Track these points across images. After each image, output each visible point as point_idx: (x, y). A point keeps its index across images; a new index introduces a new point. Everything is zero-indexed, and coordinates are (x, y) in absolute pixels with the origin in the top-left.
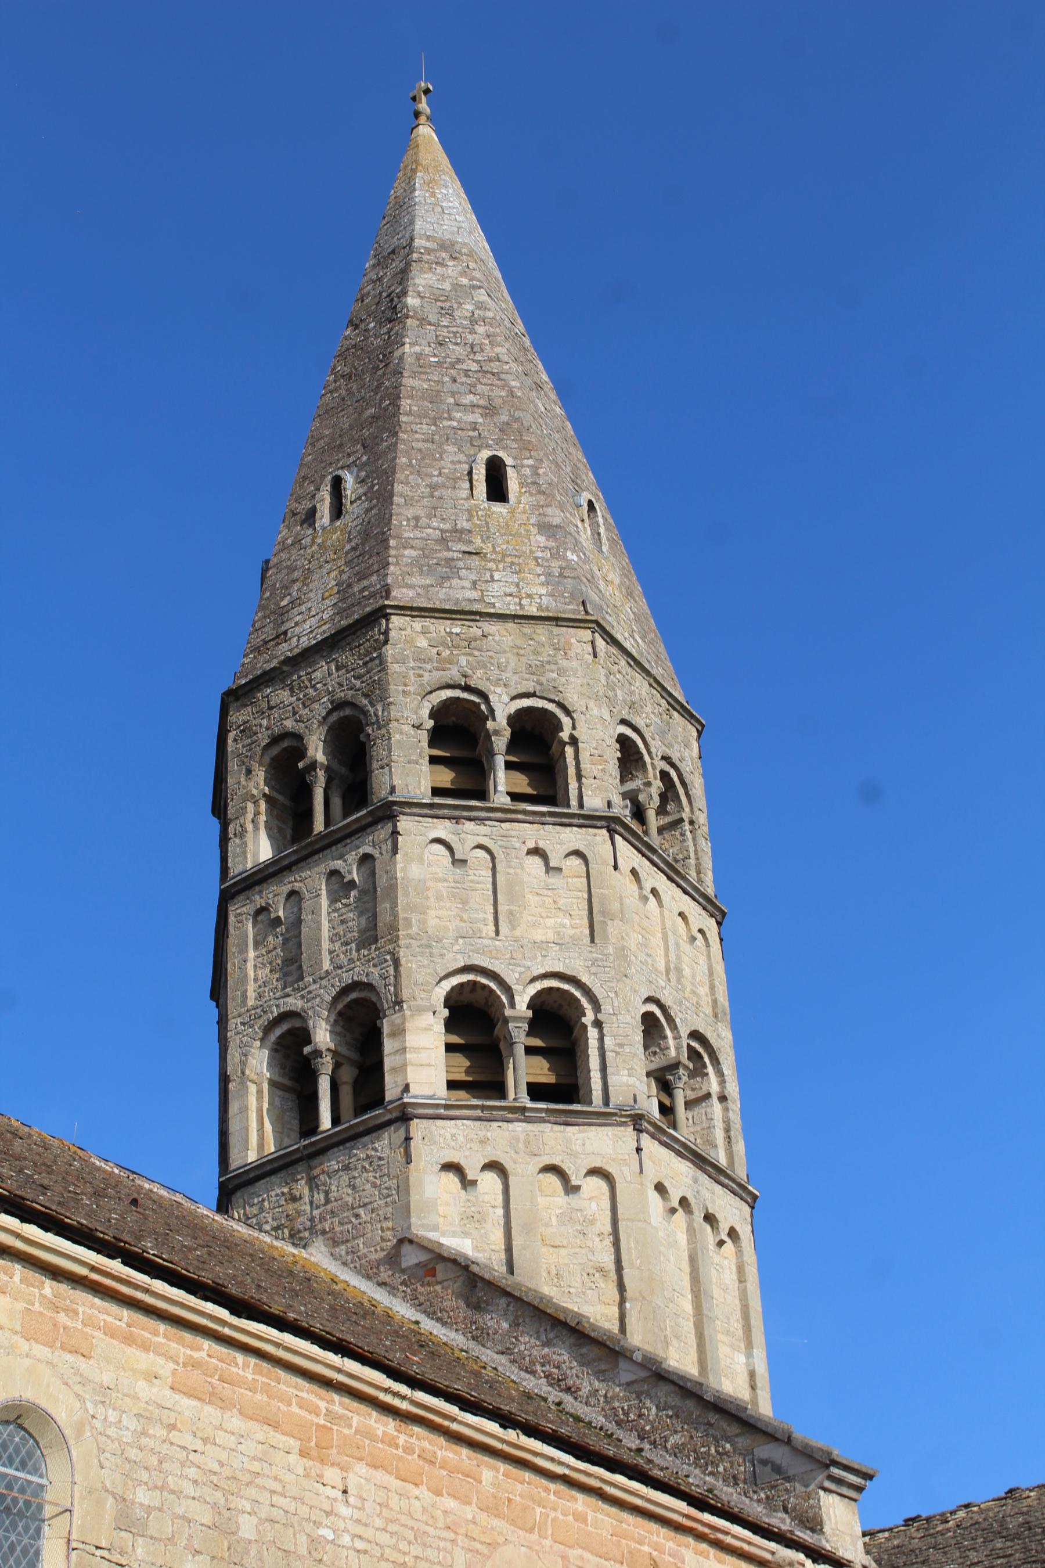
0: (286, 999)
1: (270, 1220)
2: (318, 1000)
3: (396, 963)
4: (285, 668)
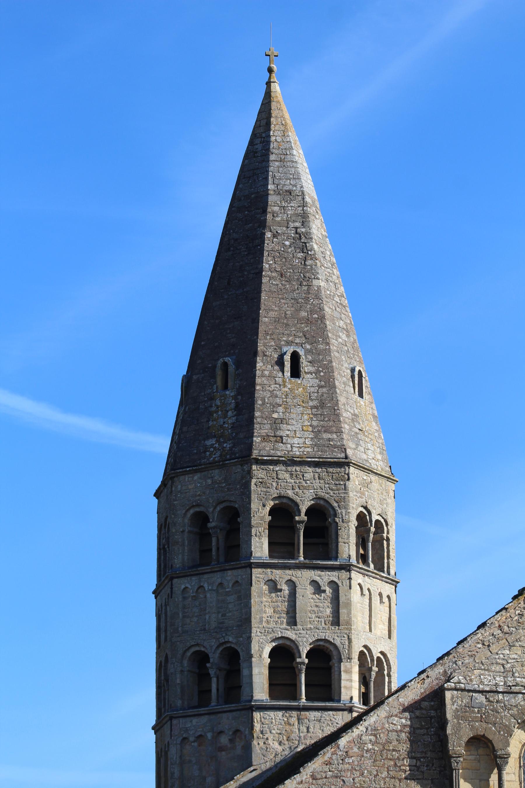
0: (287, 631)
1: (276, 729)
2: (305, 639)
3: (350, 640)
4: (288, 462)
